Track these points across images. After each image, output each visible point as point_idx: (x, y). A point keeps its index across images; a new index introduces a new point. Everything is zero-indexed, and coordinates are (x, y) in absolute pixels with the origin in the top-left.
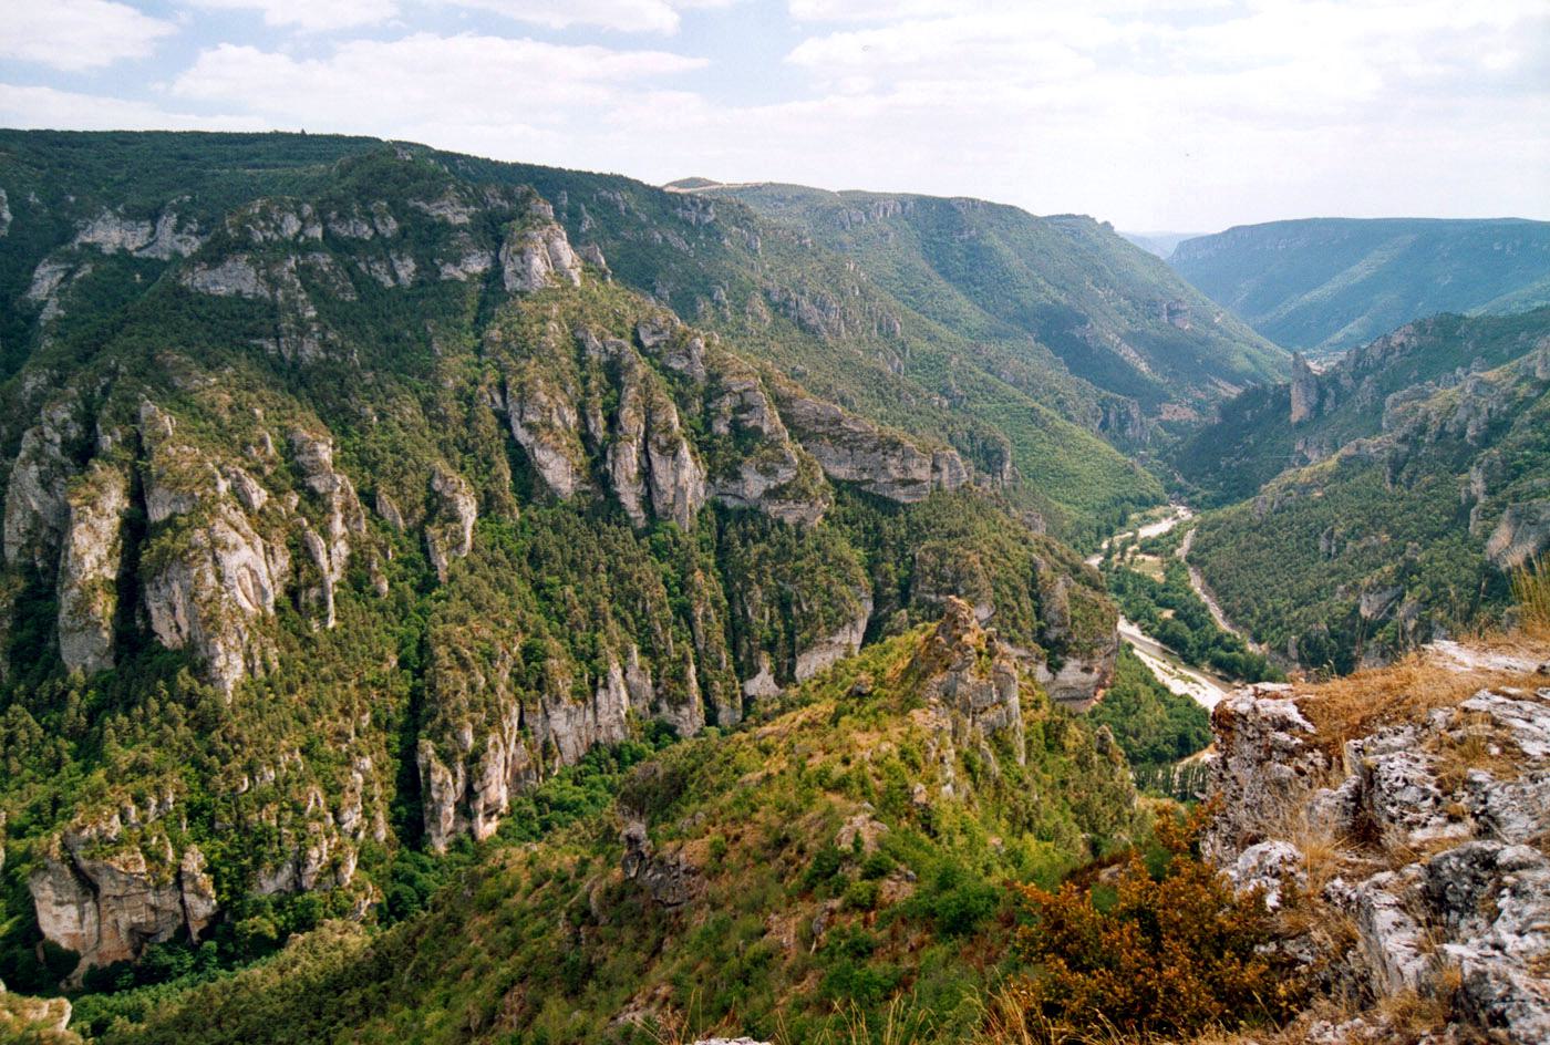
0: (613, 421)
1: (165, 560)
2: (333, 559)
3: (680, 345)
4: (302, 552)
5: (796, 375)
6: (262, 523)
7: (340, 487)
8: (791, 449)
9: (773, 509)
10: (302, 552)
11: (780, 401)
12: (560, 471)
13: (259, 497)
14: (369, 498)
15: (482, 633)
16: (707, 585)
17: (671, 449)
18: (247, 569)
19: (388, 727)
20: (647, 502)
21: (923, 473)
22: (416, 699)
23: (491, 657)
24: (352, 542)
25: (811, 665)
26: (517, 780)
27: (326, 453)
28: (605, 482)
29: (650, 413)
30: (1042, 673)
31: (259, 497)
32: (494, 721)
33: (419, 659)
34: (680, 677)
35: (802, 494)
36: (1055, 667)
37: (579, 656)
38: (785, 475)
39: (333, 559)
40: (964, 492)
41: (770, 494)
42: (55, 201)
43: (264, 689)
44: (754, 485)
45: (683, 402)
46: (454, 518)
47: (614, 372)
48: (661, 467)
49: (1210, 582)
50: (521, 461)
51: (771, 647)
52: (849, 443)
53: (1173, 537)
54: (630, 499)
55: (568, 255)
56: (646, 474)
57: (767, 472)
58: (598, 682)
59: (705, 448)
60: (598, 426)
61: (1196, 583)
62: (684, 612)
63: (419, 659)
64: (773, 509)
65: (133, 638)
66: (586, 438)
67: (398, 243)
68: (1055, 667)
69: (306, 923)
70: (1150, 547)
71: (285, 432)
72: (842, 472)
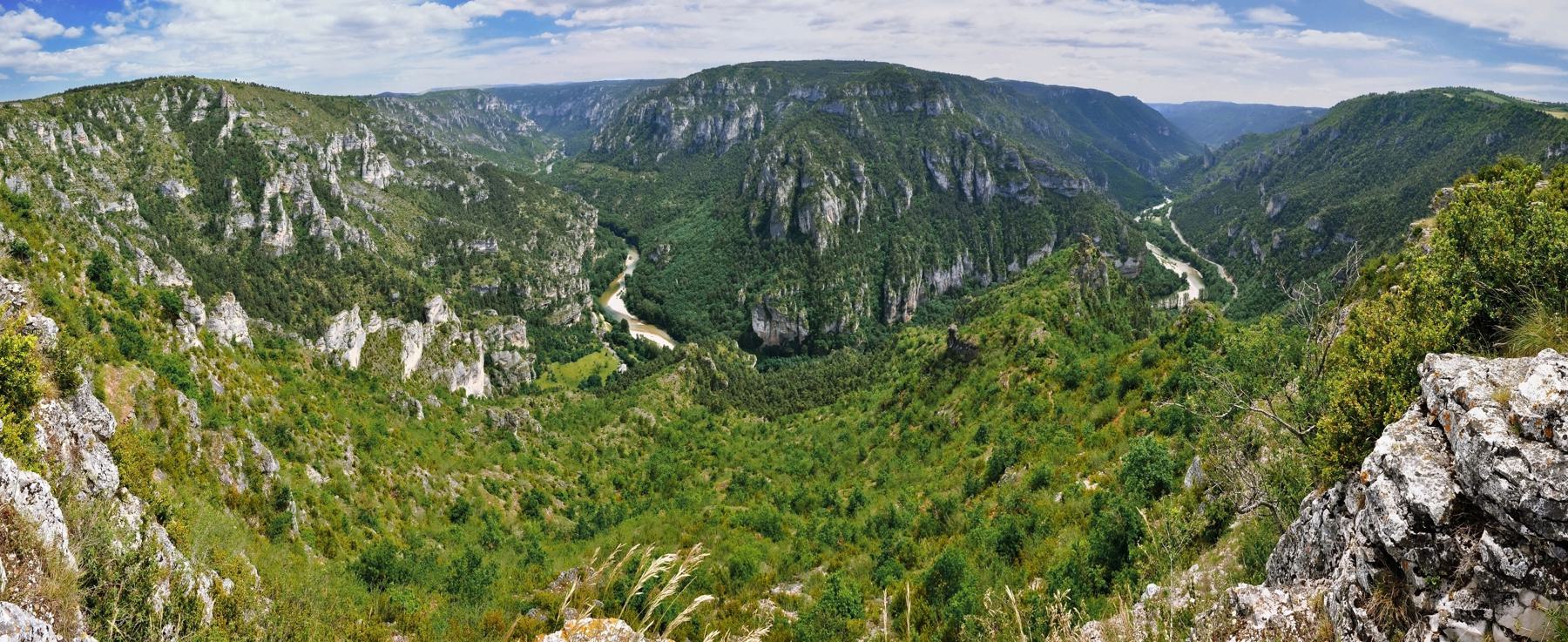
0: (963, 162)
1: (804, 204)
2: (861, 206)
3: (988, 135)
4: (850, 204)
5: (1031, 149)
6: (839, 192)
7: (866, 181)
8: (1028, 176)
9: (1021, 198)
10: (850, 204)
11: (1024, 157)
12: (943, 181)
13: (837, 182)
14: (875, 186)
15: (912, 242)
16: (995, 226)
17: (983, 174)
18: (833, 208)
19: (876, 272)
20: (974, 193)
21: (1075, 186)
22: (887, 264)
23: (914, 249)
24: (868, 200)
25: (1034, 258)
26: (920, 298)
27: (862, 169)
28: (959, 185)
29: (976, 160)
30: (1118, 263)
31: (837, 182)
32: (913, 274)
33: (887, 249)
34: (984, 262)
35: (1032, 193)
36: (1124, 261)
37: (948, 251)
38: (1026, 185)
39: (861, 206)
40: (1091, 193)
41: (1020, 192)
42: (784, 82)
43: (834, 252)
44: (1014, 190)
45: (988, 156)
46: (905, 195)
47: (964, 144)
48: (979, 180)
49: (1178, 226)
50: (931, 177)
51: (1018, 252)
52: (1051, 174)
53: (1165, 210)
54: (968, 193)
55: (949, 104)
56: (974, 182)
57: (1019, 184)
58: (953, 261)
59: (995, 173)
60: (958, 164)
61: (1173, 226)
62: (987, 238)
63: (887, 249)
64: (1021, 198)
65: (794, 229)
66: (954, 169)
67: (891, 98)
68: (1124, 261)
69: (839, 347)
70: (1157, 213)
71: (848, 160)
72: (1046, 185)
